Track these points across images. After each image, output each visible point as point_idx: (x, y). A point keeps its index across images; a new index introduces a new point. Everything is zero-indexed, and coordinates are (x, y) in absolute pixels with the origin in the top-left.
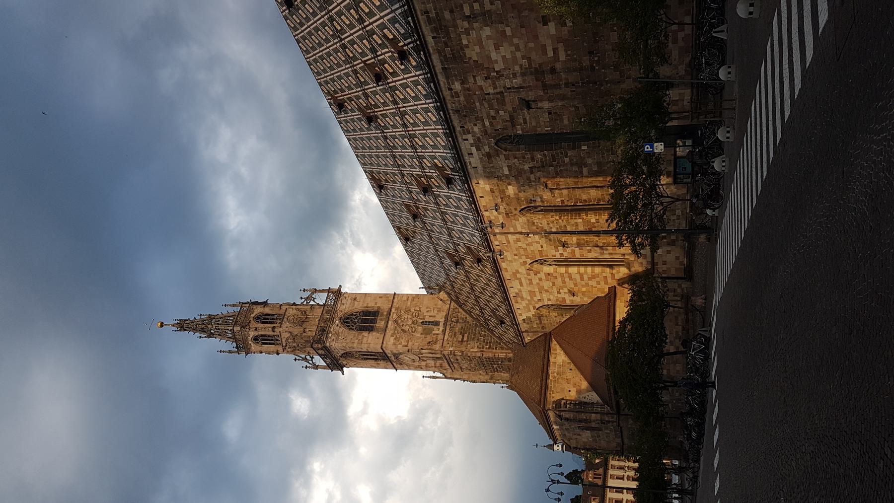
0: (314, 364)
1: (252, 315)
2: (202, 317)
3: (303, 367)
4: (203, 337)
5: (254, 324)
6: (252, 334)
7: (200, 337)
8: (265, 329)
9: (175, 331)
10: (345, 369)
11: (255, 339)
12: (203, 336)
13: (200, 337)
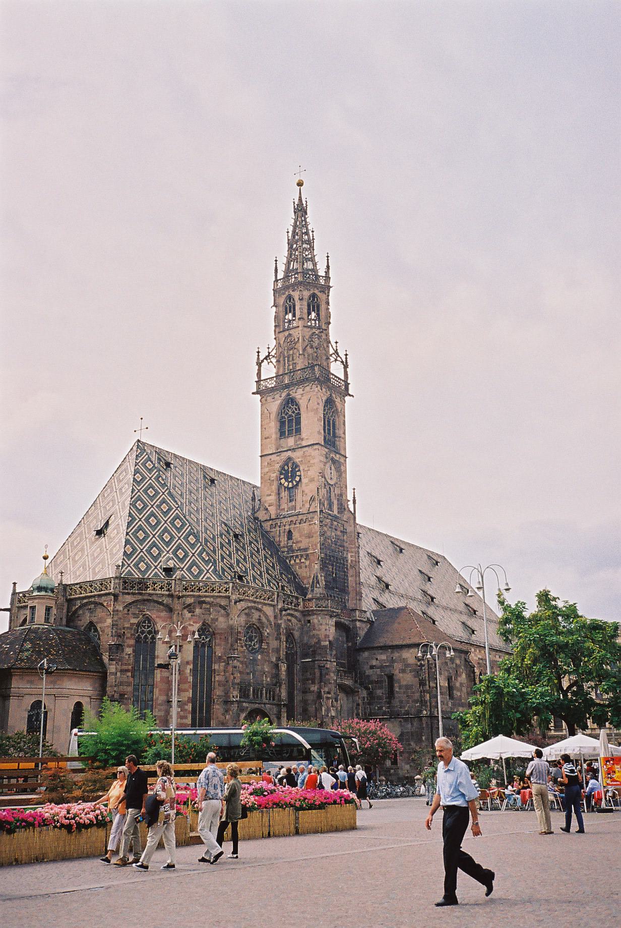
0: (263, 361)
1: (316, 292)
2: (311, 234)
3: (258, 348)
4: (288, 235)
5: (306, 294)
6: (296, 295)
7: (288, 232)
8: (301, 307)
9: (294, 202)
10: (258, 397)
11: (290, 297)
12: (290, 234)
13: (288, 232)
